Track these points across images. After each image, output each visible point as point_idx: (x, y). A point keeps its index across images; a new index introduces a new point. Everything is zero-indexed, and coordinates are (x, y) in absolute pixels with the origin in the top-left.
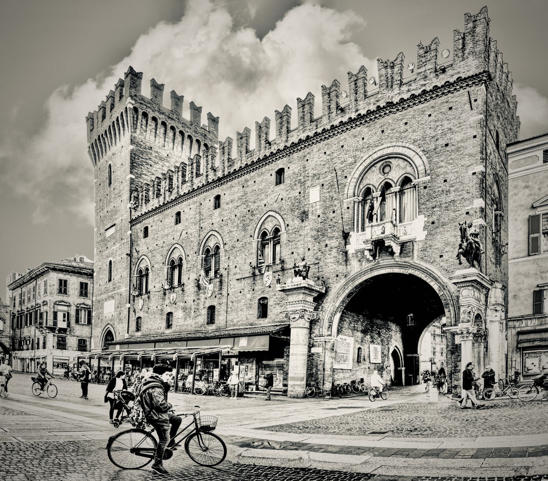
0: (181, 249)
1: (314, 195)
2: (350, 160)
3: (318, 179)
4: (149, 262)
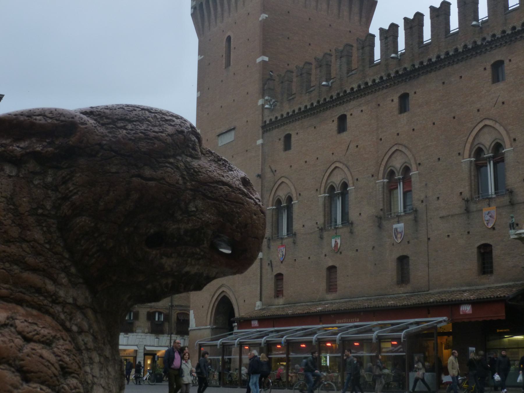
0: (346, 170)
4: (292, 188)
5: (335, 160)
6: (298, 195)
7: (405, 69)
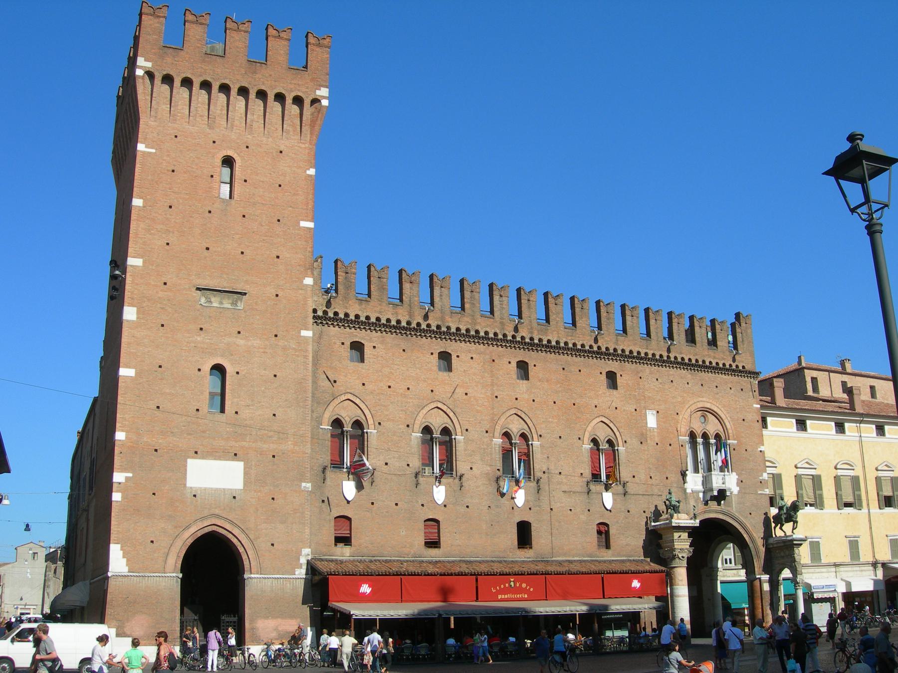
1: (652, 421)
2: (680, 399)
3: (653, 403)
5: (437, 398)
6: (377, 424)
7: (523, 338)
